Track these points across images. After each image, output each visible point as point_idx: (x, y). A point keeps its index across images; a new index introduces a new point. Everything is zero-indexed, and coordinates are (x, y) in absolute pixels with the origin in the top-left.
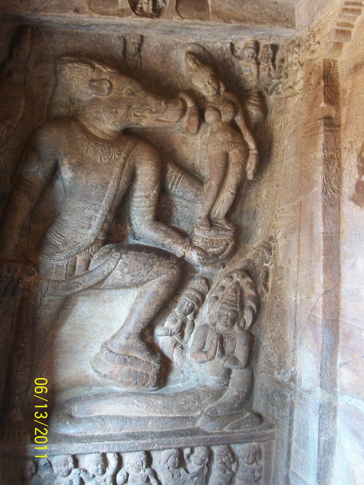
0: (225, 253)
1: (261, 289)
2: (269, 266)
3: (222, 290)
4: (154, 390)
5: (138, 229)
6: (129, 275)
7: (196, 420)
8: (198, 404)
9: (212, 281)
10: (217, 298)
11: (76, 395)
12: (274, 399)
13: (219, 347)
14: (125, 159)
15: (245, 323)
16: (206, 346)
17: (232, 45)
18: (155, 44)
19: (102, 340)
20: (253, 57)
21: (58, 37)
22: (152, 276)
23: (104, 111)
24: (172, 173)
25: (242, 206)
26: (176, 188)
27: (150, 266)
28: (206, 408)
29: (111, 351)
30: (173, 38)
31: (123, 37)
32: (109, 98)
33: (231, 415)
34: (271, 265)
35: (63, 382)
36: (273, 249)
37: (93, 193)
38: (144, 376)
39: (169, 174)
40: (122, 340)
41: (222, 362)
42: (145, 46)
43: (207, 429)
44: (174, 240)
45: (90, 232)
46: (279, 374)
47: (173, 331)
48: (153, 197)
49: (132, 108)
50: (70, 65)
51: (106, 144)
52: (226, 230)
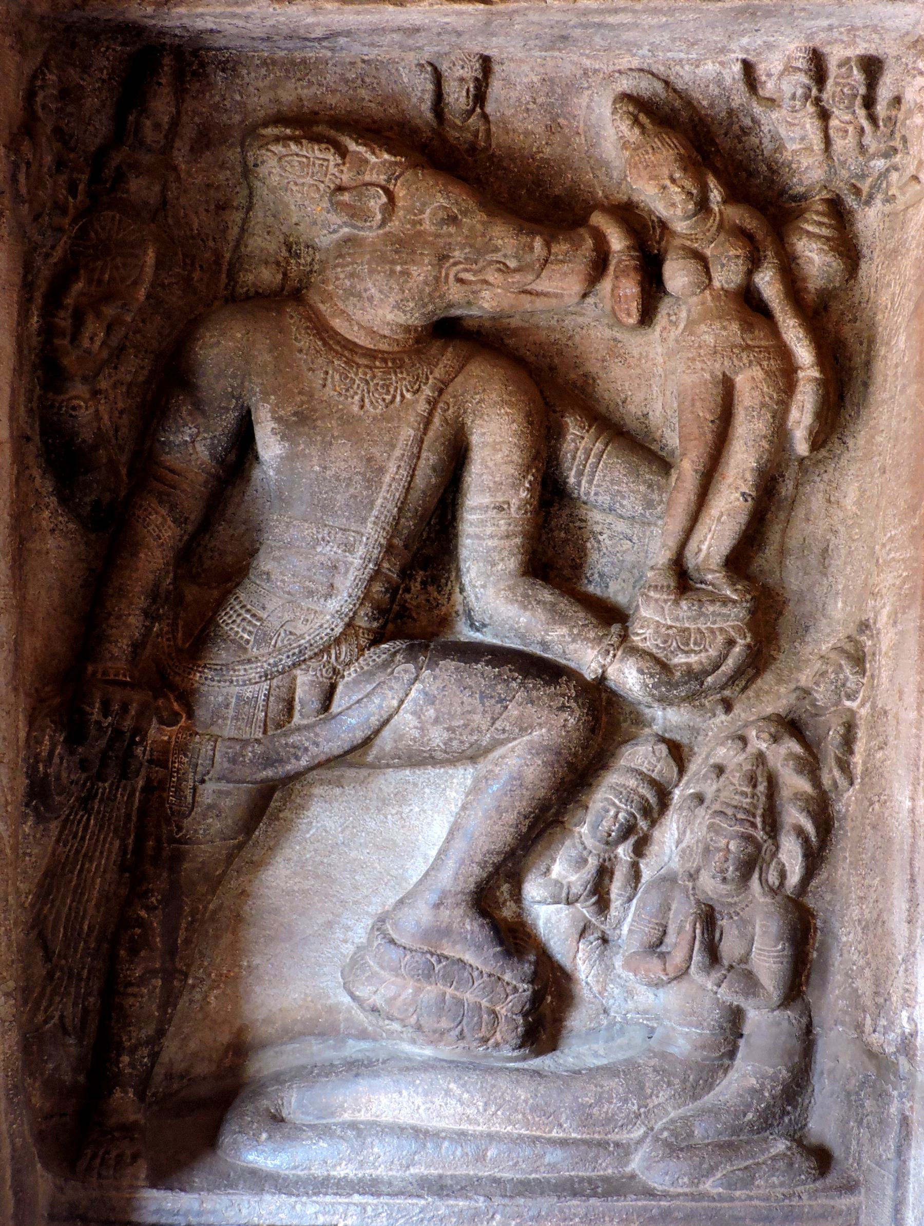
0: (723, 668)
1: (830, 774)
2: (859, 707)
3: (714, 776)
4: (515, 1060)
5: (477, 598)
6: (440, 727)
7: (628, 1154)
8: (636, 1107)
9: (691, 749)
10: (700, 799)
11: (302, 1060)
12: (862, 1106)
13: (702, 942)
14: (433, 404)
15: (783, 875)
17: (748, 68)
18: (525, 80)
19: (375, 908)
20: (807, 97)
21: (253, 75)
22: (504, 731)
23: (371, 272)
25: (784, 531)
26: (590, 482)
27: (497, 702)
28: (661, 1119)
29: (392, 941)
30: (575, 58)
31: (431, 64)
32: (387, 234)
33: (730, 1145)
34: (863, 705)
35: (267, 1021)
36: (868, 658)
37: (340, 499)
38: (485, 1016)
40: (421, 913)
41: (709, 985)
42: (496, 88)
43: (657, 1181)
44: (575, 631)
45: (333, 605)
46: (874, 1031)
47: (574, 890)
48: (519, 508)
49: (451, 261)
50: (278, 149)
51: (377, 363)
52: (726, 601)
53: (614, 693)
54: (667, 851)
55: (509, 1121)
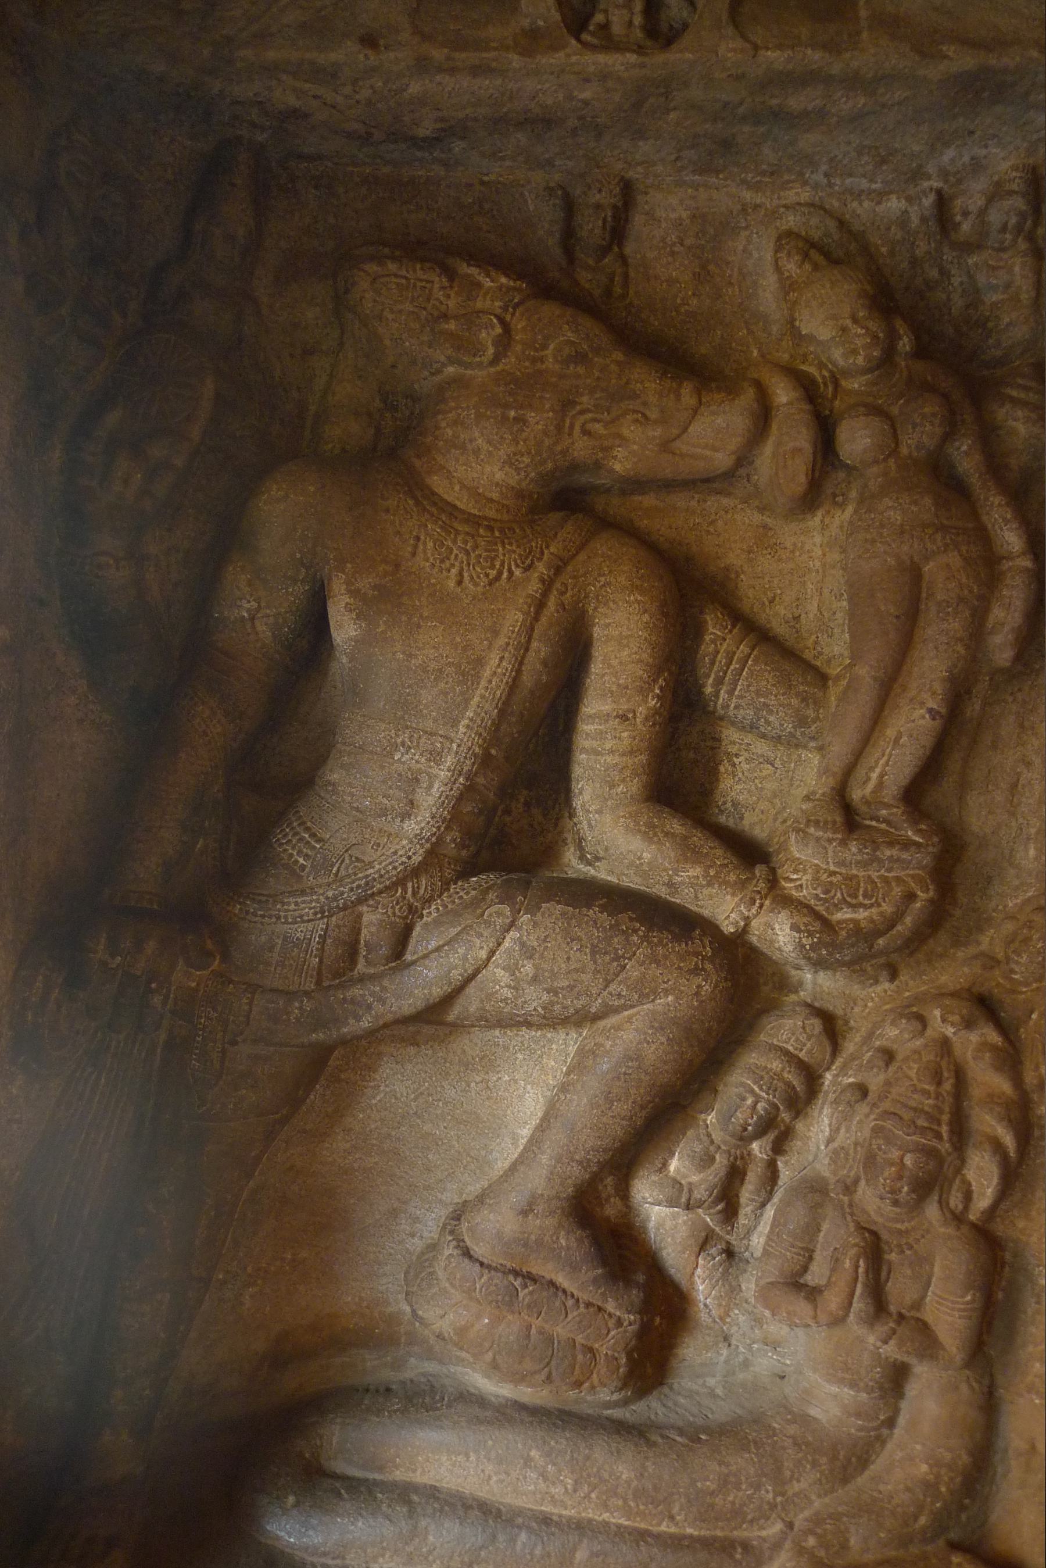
0: (899, 928)
3: (882, 1064)
4: (616, 1405)
5: (590, 825)
8: (770, 1496)
9: (847, 1023)
10: (862, 1091)
13: (865, 1285)
14: (548, 585)
15: (968, 1197)
16: (814, 1267)
17: (942, 202)
18: (673, 216)
19: (451, 1196)
20: (1019, 229)
23: (479, 417)
24: (717, 638)
26: (731, 693)
27: (613, 960)
28: (802, 1510)
29: (467, 1253)
31: (561, 187)
37: (426, 696)
38: (580, 1357)
39: (707, 648)
41: (871, 1339)
42: (638, 220)
44: (712, 873)
45: (411, 826)
47: (697, 1195)
48: (646, 719)
49: (578, 408)
50: (373, 268)
51: (481, 531)
52: (907, 845)
53: (753, 949)
54: (813, 1149)
55: (606, 1507)
